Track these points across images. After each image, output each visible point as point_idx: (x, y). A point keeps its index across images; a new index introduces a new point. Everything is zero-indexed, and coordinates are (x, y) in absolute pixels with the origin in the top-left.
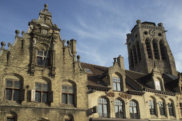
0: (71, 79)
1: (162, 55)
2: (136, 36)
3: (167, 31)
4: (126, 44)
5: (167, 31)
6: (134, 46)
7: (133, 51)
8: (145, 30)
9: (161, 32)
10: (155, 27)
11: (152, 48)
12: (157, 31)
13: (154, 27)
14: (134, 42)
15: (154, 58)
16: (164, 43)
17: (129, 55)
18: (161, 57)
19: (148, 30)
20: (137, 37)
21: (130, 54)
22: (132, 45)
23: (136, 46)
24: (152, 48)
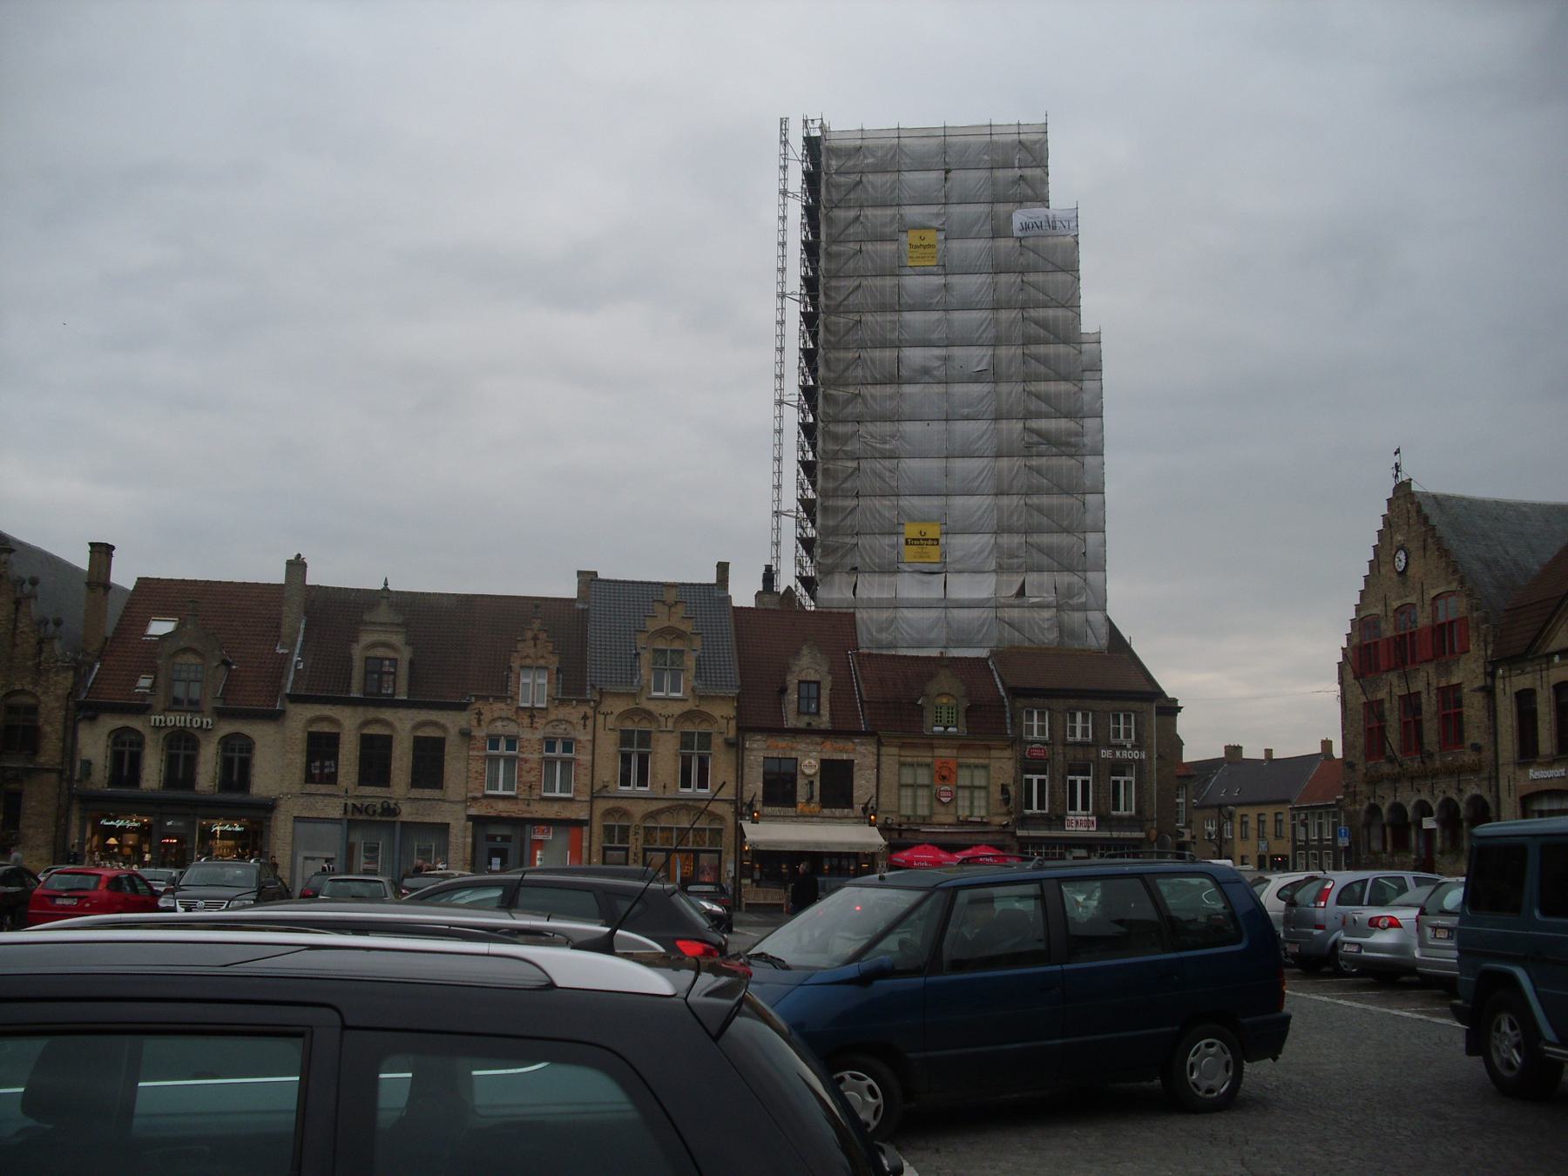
0: (29, 687)
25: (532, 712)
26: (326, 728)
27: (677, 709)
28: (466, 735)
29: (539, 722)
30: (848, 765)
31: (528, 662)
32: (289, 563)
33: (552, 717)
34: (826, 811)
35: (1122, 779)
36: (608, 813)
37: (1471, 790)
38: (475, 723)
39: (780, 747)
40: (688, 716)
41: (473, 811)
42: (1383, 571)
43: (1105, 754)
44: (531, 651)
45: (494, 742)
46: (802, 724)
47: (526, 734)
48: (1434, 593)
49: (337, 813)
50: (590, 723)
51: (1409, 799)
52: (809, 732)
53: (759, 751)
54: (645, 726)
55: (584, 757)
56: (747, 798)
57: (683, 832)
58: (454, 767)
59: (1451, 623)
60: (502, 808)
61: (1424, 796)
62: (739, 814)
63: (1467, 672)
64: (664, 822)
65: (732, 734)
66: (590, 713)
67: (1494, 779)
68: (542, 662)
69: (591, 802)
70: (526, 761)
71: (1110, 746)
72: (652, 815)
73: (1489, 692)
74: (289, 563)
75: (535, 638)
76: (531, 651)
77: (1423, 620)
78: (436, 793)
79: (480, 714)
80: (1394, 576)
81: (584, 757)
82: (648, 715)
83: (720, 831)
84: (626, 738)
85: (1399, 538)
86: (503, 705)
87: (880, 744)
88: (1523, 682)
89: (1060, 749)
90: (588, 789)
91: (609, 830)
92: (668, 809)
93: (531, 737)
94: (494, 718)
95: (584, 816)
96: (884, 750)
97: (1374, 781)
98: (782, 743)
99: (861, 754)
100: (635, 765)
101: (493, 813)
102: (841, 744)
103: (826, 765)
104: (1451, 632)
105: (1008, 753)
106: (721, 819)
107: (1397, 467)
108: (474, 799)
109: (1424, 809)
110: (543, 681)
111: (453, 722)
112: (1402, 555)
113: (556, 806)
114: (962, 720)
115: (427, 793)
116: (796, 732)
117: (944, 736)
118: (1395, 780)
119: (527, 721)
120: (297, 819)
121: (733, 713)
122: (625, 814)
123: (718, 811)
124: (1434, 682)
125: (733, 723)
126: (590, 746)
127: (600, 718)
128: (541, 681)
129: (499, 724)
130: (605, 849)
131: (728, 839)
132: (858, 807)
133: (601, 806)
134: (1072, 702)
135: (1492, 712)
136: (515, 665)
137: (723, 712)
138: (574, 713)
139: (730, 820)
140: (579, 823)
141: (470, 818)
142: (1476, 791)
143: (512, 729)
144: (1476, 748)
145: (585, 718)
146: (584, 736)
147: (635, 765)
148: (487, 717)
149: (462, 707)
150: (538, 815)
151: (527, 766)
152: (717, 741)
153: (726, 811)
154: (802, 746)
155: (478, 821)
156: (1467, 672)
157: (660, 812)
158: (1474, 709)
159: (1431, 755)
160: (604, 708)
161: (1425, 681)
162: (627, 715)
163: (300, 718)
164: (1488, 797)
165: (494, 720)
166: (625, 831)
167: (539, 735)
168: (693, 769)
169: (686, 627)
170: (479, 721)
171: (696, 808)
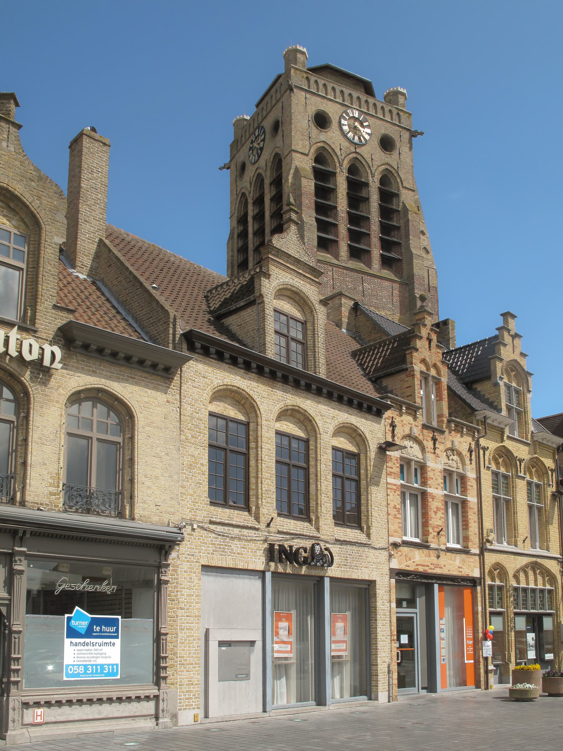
1: (386, 245)
2: (276, 126)
3: (422, 134)
5: (422, 134)
6: (259, 180)
7: (250, 207)
8: (318, 104)
9: (392, 132)
10: (371, 100)
13: (364, 97)
14: (262, 162)
16: (403, 192)
17: (235, 224)
18: (376, 252)
20: (280, 132)
21: (239, 222)
22: (250, 172)
23: (267, 182)
79: (393, 426)
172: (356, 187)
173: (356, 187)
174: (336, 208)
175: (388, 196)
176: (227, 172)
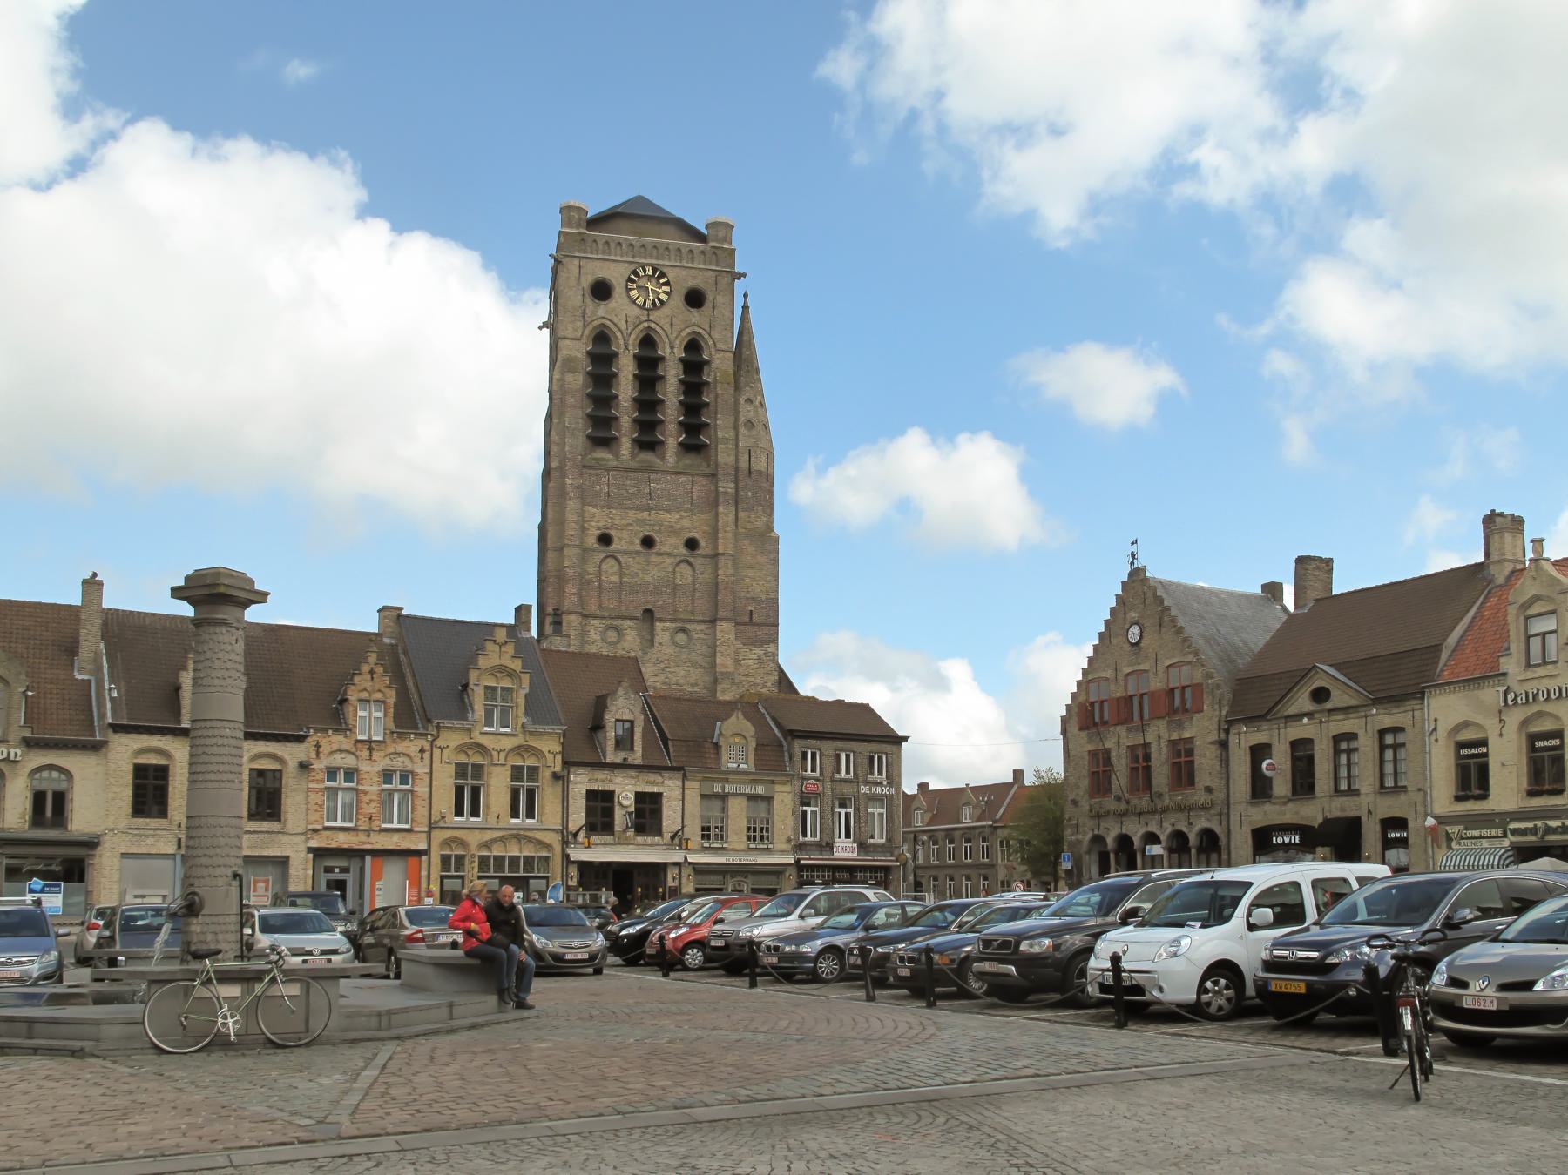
3: (744, 275)
4: (545, 325)
11: (626, 389)
12: (685, 276)
15: (626, 446)
19: (616, 274)
24: (626, 389)
25: (370, 744)
26: (154, 760)
27: (509, 743)
28: (304, 766)
29: (378, 755)
30: (656, 798)
31: (365, 695)
32: (85, 582)
33: (391, 750)
34: (640, 839)
35: (809, 809)
36: (446, 843)
37: (1202, 823)
38: (313, 755)
39: (600, 781)
40: (519, 750)
41: (314, 844)
42: (1114, 641)
43: (864, 789)
44: (368, 685)
45: (332, 773)
46: (619, 760)
47: (365, 767)
48: (1168, 663)
49: (171, 848)
50: (427, 755)
51: (1136, 831)
52: (625, 766)
53: (582, 782)
54: (477, 760)
55: (422, 789)
56: (573, 827)
57: (514, 861)
58: (294, 801)
59: (1183, 688)
60: (342, 841)
61: (1153, 828)
62: (565, 843)
63: (1201, 729)
64: (497, 851)
65: (558, 768)
66: (427, 747)
67: (1225, 815)
68: (378, 696)
69: (429, 834)
70: (366, 793)
71: (867, 783)
72: (487, 845)
73: (1223, 745)
74: (85, 582)
75: (372, 672)
76: (368, 685)
77: (1156, 684)
78: (274, 826)
79: (318, 746)
80: (1127, 646)
81: (422, 789)
82: (481, 749)
83: (547, 859)
84: (461, 771)
85: (1133, 615)
86: (341, 738)
87: (685, 777)
88: (1259, 737)
89: (828, 785)
90: (426, 821)
91: (445, 860)
92: (502, 839)
93: (370, 768)
94: (331, 749)
95: (423, 846)
96: (688, 784)
97: (1098, 816)
98: (601, 775)
99: (668, 787)
100: (468, 799)
101: (334, 845)
102: (652, 777)
103: (640, 797)
104: (1183, 695)
105: (788, 788)
106: (548, 847)
107: (1133, 556)
108: (315, 831)
109: (1152, 838)
110: (380, 714)
111: (292, 754)
112: (1135, 630)
113: (396, 837)
114: (751, 757)
115: (266, 825)
116: (614, 766)
117: (737, 772)
118: (1121, 815)
119: (366, 753)
120: (124, 855)
121: (559, 749)
122: (463, 843)
123: (547, 840)
124: (1165, 735)
125: (559, 758)
126: (427, 780)
127: (437, 751)
128: (376, 714)
129: (338, 756)
130: (442, 878)
131: (556, 864)
132: (667, 836)
133: (439, 836)
134: (839, 744)
135: (1225, 761)
136: (353, 696)
137: (550, 746)
138: (412, 746)
139: (558, 848)
140: (418, 853)
141: (310, 850)
142: (1206, 824)
143: (350, 761)
144: (1209, 790)
145: (422, 751)
146: (421, 769)
147: (468, 799)
148: (325, 749)
149: (300, 739)
150: (378, 846)
151: (366, 799)
152: (546, 774)
153: (554, 840)
154: (619, 780)
155: (319, 853)
156: (1201, 729)
157: (494, 840)
158: (1206, 760)
159: (1160, 795)
160: (439, 743)
161: (1158, 735)
162: (462, 749)
163: (126, 751)
164: (1217, 829)
165: (332, 753)
166: (460, 859)
167: (378, 767)
168: (523, 801)
169: (517, 665)
170: (318, 753)
171: (519, 836)
172: (648, 363)
173: (648, 363)
174: (616, 397)
175: (694, 362)
176: (546, 331)
